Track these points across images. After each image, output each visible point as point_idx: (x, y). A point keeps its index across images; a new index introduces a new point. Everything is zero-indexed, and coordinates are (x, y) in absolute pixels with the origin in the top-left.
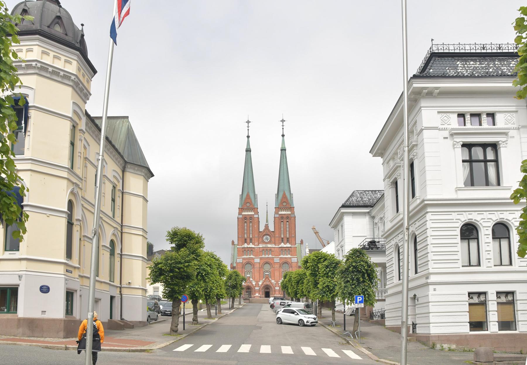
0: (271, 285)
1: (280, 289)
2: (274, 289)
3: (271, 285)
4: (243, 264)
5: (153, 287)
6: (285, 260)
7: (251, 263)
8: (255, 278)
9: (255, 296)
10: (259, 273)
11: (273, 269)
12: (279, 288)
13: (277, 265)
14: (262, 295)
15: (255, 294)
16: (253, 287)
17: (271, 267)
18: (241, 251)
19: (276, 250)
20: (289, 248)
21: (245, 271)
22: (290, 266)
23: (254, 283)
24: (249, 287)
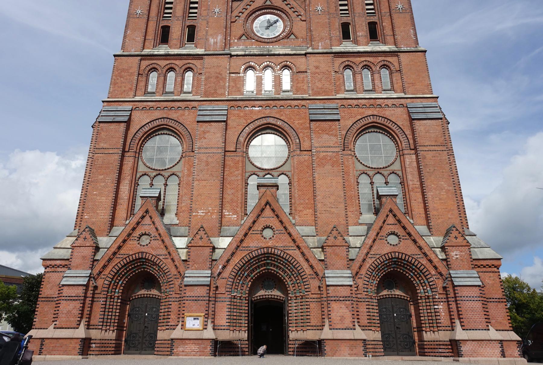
0: (296, 254)
1: (360, 282)
2: (314, 284)
3: (296, 254)
4: (133, 130)
5: (44, 260)
6: (370, 112)
7: (180, 128)
9: (177, 333)
10: (217, 183)
11: (305, 157)
12: (355, 276)
13: (325, 137)
14: (233, 324)
15: (181, 318)
16: (168, 265)
18: (135, 70)
19: (317, 67)
20: (389, 59)
21: (142, 168)
22: (404, 144)
23: (180, 242)
24: (153, 271)
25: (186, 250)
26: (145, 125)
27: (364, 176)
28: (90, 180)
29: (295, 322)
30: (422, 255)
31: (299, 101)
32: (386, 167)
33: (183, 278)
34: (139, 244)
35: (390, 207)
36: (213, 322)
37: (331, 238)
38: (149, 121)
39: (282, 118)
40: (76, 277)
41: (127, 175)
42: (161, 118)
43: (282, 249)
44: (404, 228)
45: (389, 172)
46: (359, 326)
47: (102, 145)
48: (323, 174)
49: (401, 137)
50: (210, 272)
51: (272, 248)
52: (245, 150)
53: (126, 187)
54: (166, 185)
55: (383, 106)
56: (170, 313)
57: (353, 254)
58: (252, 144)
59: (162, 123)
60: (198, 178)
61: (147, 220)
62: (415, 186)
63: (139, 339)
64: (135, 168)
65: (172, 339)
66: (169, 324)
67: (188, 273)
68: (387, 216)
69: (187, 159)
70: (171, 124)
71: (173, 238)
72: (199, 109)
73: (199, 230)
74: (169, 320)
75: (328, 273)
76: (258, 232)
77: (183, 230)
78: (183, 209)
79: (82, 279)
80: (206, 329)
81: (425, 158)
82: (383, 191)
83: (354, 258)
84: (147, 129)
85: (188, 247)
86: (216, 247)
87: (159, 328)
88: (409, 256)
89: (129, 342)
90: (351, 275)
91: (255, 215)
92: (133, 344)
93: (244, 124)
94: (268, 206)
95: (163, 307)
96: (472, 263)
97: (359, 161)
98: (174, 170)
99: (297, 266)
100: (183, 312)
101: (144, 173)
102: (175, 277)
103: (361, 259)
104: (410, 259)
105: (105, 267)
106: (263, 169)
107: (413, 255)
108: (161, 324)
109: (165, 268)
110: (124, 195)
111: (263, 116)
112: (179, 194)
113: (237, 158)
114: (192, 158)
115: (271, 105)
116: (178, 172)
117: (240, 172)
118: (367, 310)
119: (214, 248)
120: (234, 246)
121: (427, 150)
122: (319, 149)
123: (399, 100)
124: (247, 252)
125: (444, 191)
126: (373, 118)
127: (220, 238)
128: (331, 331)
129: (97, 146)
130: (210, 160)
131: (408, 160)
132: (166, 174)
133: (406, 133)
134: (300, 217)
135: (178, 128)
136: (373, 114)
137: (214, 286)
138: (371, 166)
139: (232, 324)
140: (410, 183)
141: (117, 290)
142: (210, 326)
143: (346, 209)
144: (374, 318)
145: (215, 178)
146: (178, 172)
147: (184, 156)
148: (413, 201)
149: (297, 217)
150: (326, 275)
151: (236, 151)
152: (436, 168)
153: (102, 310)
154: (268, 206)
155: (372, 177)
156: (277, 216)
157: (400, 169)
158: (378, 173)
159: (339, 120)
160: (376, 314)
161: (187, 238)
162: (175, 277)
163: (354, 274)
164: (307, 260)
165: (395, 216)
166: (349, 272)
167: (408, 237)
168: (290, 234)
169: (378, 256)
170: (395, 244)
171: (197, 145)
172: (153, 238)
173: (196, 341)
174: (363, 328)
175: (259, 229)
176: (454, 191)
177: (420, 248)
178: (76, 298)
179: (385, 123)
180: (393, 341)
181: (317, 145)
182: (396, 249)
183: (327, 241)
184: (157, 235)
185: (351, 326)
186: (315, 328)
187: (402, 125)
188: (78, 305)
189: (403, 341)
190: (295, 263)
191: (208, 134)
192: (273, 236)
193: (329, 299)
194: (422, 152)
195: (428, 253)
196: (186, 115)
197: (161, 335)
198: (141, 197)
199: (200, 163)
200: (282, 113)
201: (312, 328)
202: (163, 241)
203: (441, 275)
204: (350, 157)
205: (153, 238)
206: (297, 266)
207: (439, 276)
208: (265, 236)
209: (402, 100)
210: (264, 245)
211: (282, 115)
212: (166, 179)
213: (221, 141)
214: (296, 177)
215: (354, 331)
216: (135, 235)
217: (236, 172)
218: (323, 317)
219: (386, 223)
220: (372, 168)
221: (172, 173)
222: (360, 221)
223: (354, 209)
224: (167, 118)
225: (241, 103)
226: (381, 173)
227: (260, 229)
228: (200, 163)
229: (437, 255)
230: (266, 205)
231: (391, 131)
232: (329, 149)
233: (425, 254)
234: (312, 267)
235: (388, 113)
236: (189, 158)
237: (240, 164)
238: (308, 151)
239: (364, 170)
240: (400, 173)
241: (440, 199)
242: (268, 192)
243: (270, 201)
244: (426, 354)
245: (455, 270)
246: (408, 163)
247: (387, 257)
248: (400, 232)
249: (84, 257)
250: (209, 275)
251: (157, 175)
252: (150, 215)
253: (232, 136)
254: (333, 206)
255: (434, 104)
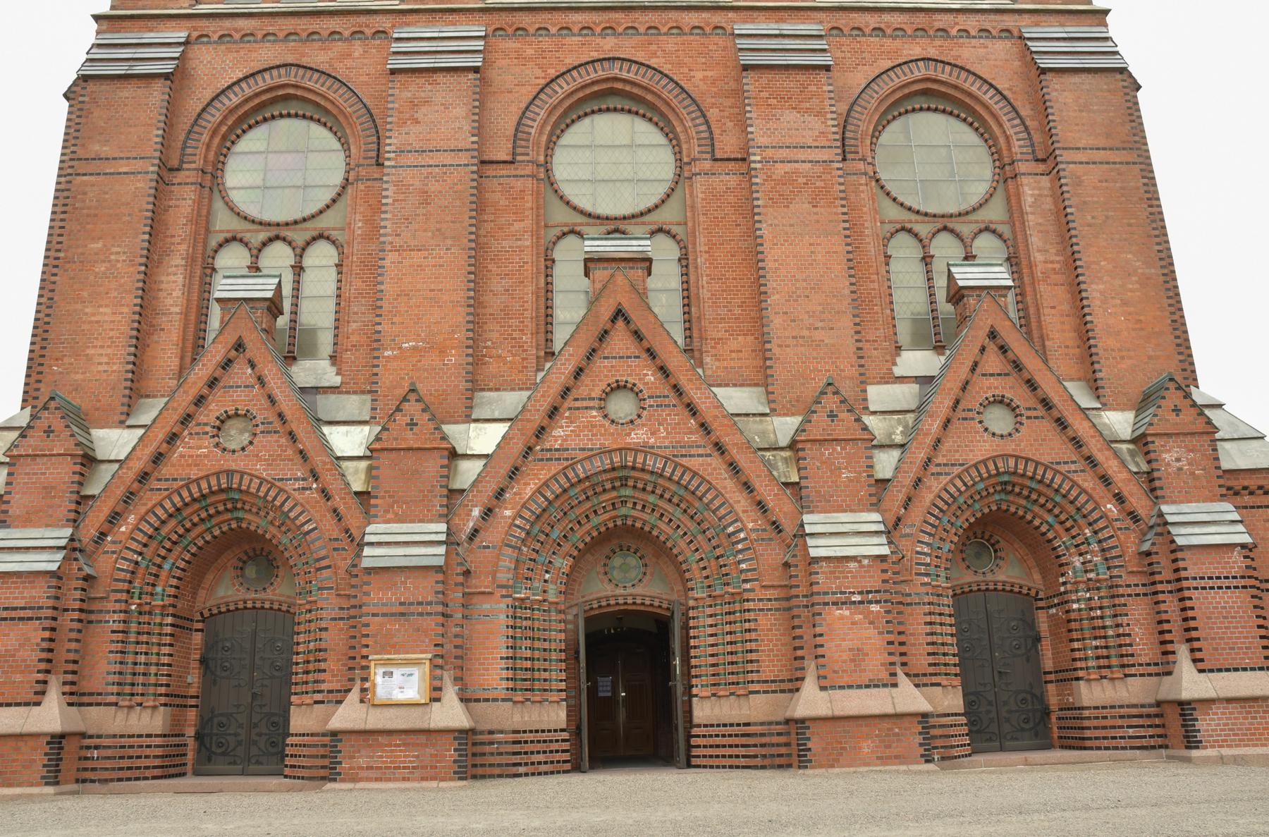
2: (772, 555)
3: (713, 467)
6: (916, 51)
7: (338, 96)
8: (375, 342)
9: (348, 715)
12: (892, 530)
13: (790, 117)
17: (693, 148)
21: (223, 222)
22: (1018, 146)
25: (363, 464)
26: (229, 87)
27: (903, 238)
28: (62, 255)
29: (711, 670)
30: (1081, 465)
31: (705, 15)
32: (967, 213)
33: (361, 545)
34: (217, 445)
35: (989, 322)
36: (457, 680)
37: (820, 418)
38: (241, 76)
39: (653, 62)
40: (28, 548)
41: (177, 240)
42: (278, 67)
43: (668, 452)
44: (1031, 384)
45: (975, 227)
46: (907, 675)
47: (97, 147)
48: (788, 229)
49: (1007, 125)
50: (443, 527)
51: (637, 451)
52: (542, 158)
53: (173, 278)
54: (298, 269)
55: (954, 32)
56: (321, 655)
57: (885, 464)
58: (563, 141)
59: (284, 80)
60: (398, 242)
61: (241, 372)
62: (1050, 266)
63: (239, 730)
64: (202, 221)
65: (334, 734)
66: (324, 687)
67: (375, 531)
68: (983, 349)
69: (362, 187)
70: (309, 84)
71: (326, 430)
72: (396, 35)
73: (405, 399)
74: (321, 676)
75: (813, 521)
76: (591, 404)
77: (354, 405)
78: (354, 339)
79: (45, 556)
80: (438, 700)
81: (1079, 183)
82: (968, 276)
83: (888, 475)
84: (235, 100)
85: (373, 452)
86: (460, 451)
87: (294, 698)
88: (1046, 467)
89: (207, 740)
90: (881, 527)
91: (583, 351)
92: (220, 745)
93: (538, 81)
94: (620, 323)
95: (301, 638)
96: (1221, 482)
97: (888, 194)
98: (325, 222)
99: (717, 503)
100: (365, 651)
101: (229, 235)
102: (336, 545)
103: (908, 480)
104: (1049, 475)
105: (115, 518)
106: (598, 217)
107: (1058, 463)
108: (299, 689)
109: (302, 519)
110: (169, 301)
111: (595, 55)
112: (339, 296)
113: (519, 184)
114: (377, 184)
115: (619, 24)
116: (334, 229)
117: (528, 223)
118: (928, 629)
119: (454, 455)
120: (518, 446)
121: (1084, 160)
122: (769, 153)
123: (998, 17)
124: (555, 468)
125: (1134, 279)
126: (927, 68)
127: (473, 425)
128: (824, 694)
129: (81, 153)
130: (433, 187)
131: (1030, 192)
132: (299, 237)
133: (1023, 113)
134: (717, 358)
135: (331, 95)
136: (924, 54)
137: (459, 570)
138: (922, 209)
139: (519, 684)
140: (1038, 257)
141: (159, 589)
142: (450, 694)
143: (858, 332)
144: (946, 649)
145: (449, 242)
146: (334, 229)
147: (351, 179)
148: (1047, 311)
149: (707, 359)
150: (808, 529)
151: (512, 162)
152: (1111, 214)
153: (114, 647)
154: (620, 323)
155: (926, 241)
156: (651, 353)
157: (1005, 217)
158: (945, 228)
159: (827, 68)
160: (949, 640)
161: (366, 429)
162: (336, 545)
163: (890, 526)
164: (747, 487)
165: (1003, 349)
166: (876, 516)
167: (1041, 412)
168: (692, 410)
169: (957, 470)
170: (1005, 433)
171: (393, 142)
172: (261, 428)
173: (412, 739)
174: (916, 680)
175: (593, 395)
176: (1162, 278)
177: (1077, 443)
178: (29, 613)
179: (959, 82)
180: (988, 712)
181: (762, 141)
182: (1010, 447)
183: (808, 426)
184: (273, 418)
185: (884, 675)
186: (773, 687)
187: (1010, 89)
188: (35, 633)
189: (1016, 711)
190: (709, 496)
191: (424, 110)
192: (639, 416)
193: (816, 599)
194: (1071, 166)
195: (1100, 457)
196: (356, 54)
197: (302, 720)
198: (218, 300)
199: (402, 197)
200: (653, 47)
201: (765, 687)
202: (292, 436)
203: (1135, 518)
204: (863, 180)
205: (261, 428)
206: (717, 503)
207: (1128, 522)
208: (612, 416)
209: (1006, 17)
210: (608, 443)
211: (654, 54)
212: (298, 251)
213: (467, 127)
214: (701, 240)
215: (894, 690)
216: (203, 419)
217: (517, 226)
218: (799, 653)
219: (978, 370)
220: (926, 214)
221: (315, 233)
222: (898, 371)
223: (880, 333)
224: (298, 66)
225: (526, 20)
226: (952, 231)
227: (596, 393)
228: (402, 197)
229: (1123, 464)
230: (614, 320)
231: (978, 108)
232: (801, 155)
233: (1091, 461)
234: (761, 506)
235: (968, 53)
236: (369, 183)
237: (529, 202)
238: (735, 159)
239: (903, 221)
240: (1004, 229)
241: (1125, 303)
242: (620, 279)
243: (627, 307)
244: (1088, 743)
245: (1174, 502)
246: (1030, 200)
247: (983, 471)
248: (1020, 397)
249: (48, 489)
250: (443, 537)
251: (271, 240)
252: (248, 356)
253: (504, 118)
254: (820, 324)
255: (1095, 31)
